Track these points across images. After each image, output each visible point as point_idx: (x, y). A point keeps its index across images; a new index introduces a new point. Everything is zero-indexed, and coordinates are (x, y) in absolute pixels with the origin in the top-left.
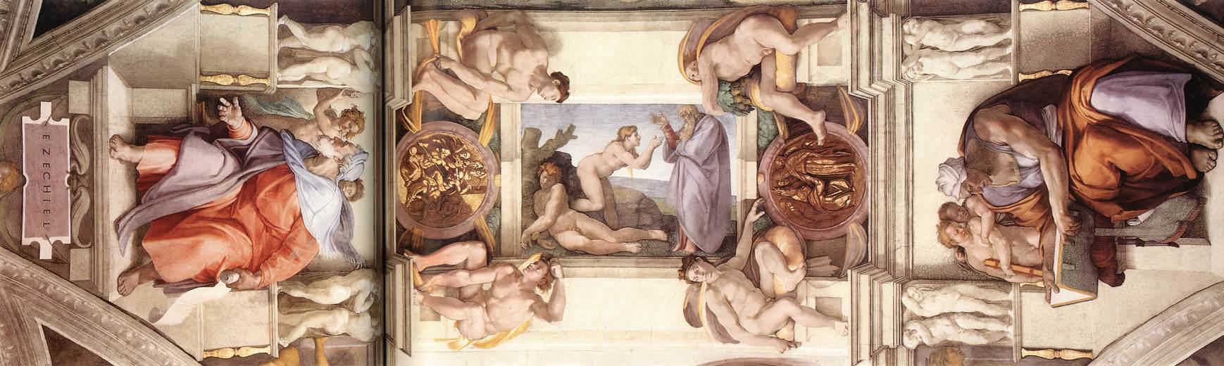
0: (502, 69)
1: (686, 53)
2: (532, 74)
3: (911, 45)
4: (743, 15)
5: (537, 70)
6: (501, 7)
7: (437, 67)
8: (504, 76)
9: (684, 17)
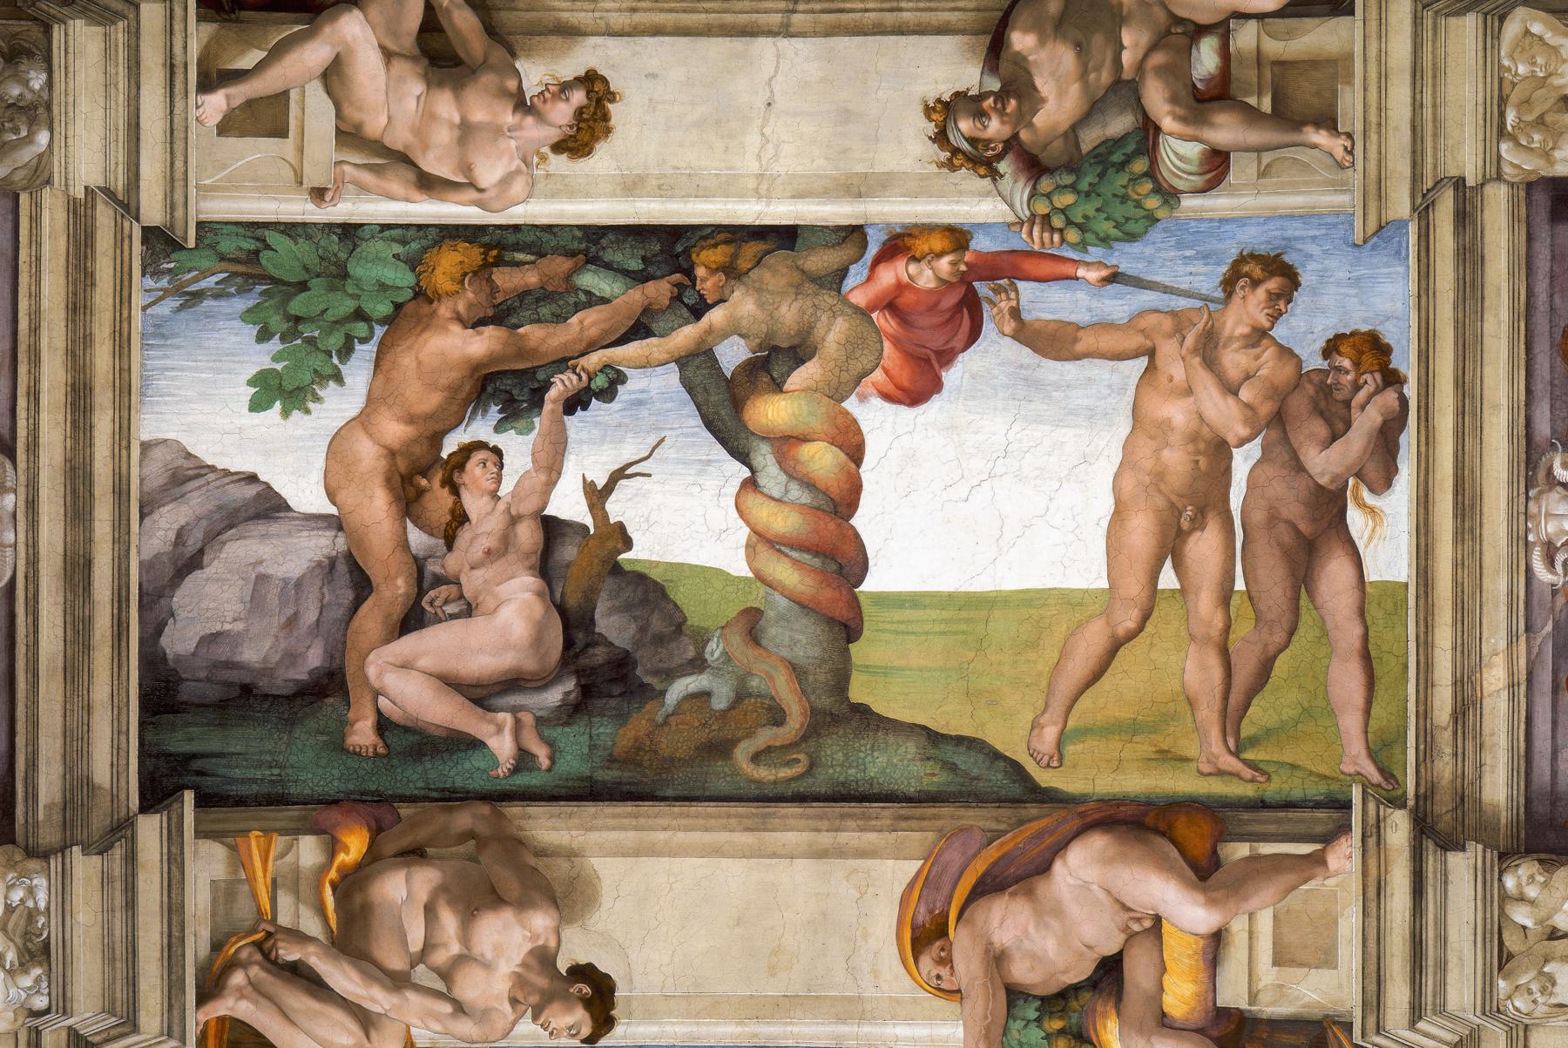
0: (440, 957)
1: (920, 919)
2: (517, 970)
3: (1524, 928)
4: (1075, 824)
5: (533, 962)
6: (435, 794)
7: (266, 956)
8: (446, 975)
9: (914, 823)
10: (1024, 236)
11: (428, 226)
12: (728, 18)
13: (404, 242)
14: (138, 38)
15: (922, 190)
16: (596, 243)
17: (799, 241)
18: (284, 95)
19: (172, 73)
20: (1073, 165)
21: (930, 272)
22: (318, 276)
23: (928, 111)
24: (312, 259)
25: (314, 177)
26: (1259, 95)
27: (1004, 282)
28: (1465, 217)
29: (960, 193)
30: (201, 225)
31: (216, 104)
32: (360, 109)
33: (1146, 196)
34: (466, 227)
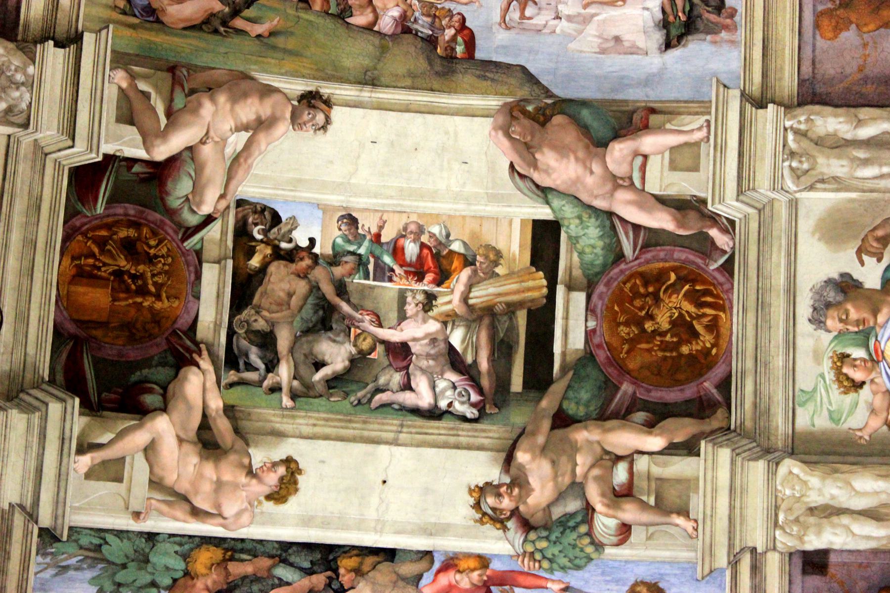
10: (519, 563)
11: (195, 536)
12: (366, 433)
13: (181, 545)
14: (46, 422)
15: (465, 534)
16: (286, 551)
17: (397, 557)
18: (122, 460)
19: (63, 443)
20: (546, 527)
21: (467, 579)
22: (133, 561)
23: (471, 491)
24: (130, 552)
25: (135, 506)
26: (649, 495)
27: (507, 587)
28: (756, 569)
29: (486, 537)
30: (71, 528)
31: (85, 461)
32: (163, 469)
33: (586, 545)
34: (215, 538)
